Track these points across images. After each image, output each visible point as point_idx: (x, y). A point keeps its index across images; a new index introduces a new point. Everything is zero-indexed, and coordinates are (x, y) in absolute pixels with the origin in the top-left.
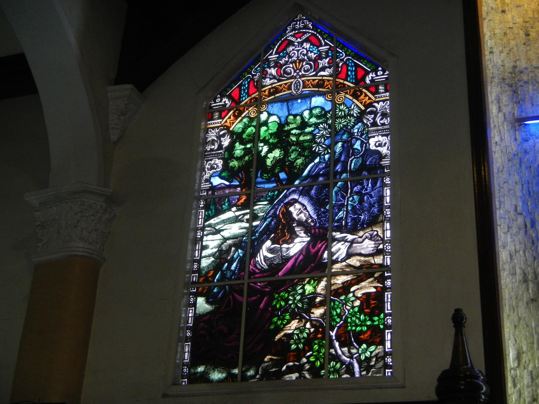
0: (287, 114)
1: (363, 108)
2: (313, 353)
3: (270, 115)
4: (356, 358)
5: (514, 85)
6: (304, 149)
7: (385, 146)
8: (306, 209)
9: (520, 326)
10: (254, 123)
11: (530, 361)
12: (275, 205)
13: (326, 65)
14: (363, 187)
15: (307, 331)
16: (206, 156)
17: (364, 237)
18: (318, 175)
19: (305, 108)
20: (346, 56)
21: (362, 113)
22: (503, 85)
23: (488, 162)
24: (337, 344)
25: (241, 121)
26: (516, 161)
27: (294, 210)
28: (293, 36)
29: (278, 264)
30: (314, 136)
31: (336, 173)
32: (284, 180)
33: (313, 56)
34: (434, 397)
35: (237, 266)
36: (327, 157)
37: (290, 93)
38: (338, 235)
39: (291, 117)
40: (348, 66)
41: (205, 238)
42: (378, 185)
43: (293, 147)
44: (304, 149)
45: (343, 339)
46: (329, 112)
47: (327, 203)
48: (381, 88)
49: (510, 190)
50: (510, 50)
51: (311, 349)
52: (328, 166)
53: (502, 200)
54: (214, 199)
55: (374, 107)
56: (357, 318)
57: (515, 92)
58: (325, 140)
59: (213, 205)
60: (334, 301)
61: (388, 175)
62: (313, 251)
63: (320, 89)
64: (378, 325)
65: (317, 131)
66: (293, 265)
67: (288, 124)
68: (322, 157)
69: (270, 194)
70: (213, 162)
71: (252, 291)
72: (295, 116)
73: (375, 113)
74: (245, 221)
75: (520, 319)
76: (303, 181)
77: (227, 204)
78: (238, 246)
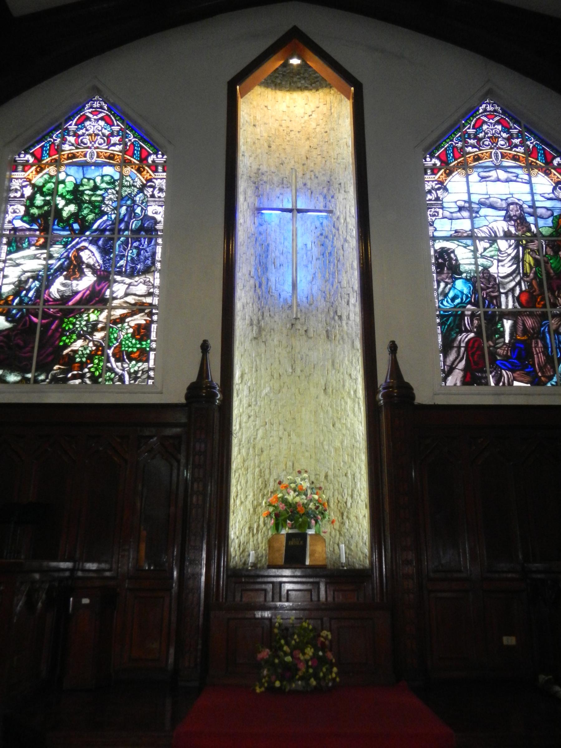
0: (82, 177)
1: (145, 182)
2: (94, 365)
3: (68, 175)
4: (127, 371)
5: (257, 183)
6: (95, 207)
7: (159, 214)
8: (94, 255)
9: (245, 356)
10: (54, 180)
11: (249, 380)
12: (69, 249)
13: (117, 142)
14: (141, 244)
15: (90, 349)
16: (8, 201)
17: (139, 281)
18: (105, 230)
19: (97, 174)
20: (134, 137)
21: (144, 186)
22: (249, 181)
23: (235, 238)
24: (112, 360)
25: (42, 176)
26: (253, 239)
27: (85, 256)
28: (91, 113)
29: (69, 296)
30: (104, 198)
31: (120, 230)
32: (77, 230)
33: (107, 133)
34: (183, 401)
35: (33, 294)
36: (113, 216)
37: (86, 160)
38: (118, 278)
39: (85, 180)
40: (134, 146)
41: (6, 269)
42: (153, 243)
43: (86, 205)
44: (95, 207)
45: (117, 356)
46: (117, 180)
47: (111, 253)
48: (160, 169)
49: (247, 259)
50: (257, 156)
51: (92, 362)
52: (113, 223)
53: (241, 266)
54: (16, 238)
55: (153, 182)
56: (129, 341)
57: (257, 188)
58: (113, 203)
59: (14, 243)
60: (112, 328)
61: (161, 236)
62: (98, 288)
63: (111, 161)
64: (145, 348)
65: (106, 194)
66: (81, 298)
67: (82, 185)
68: (109, 216)
69: (64, 240)
70: (15, 207)
71: (46, 315)
72: (89, 179)
73: (154, 187)
74: (42, 259)
75: (245, 350)
76: (92, 232)
77: (27, 244)
78: (35, 278)
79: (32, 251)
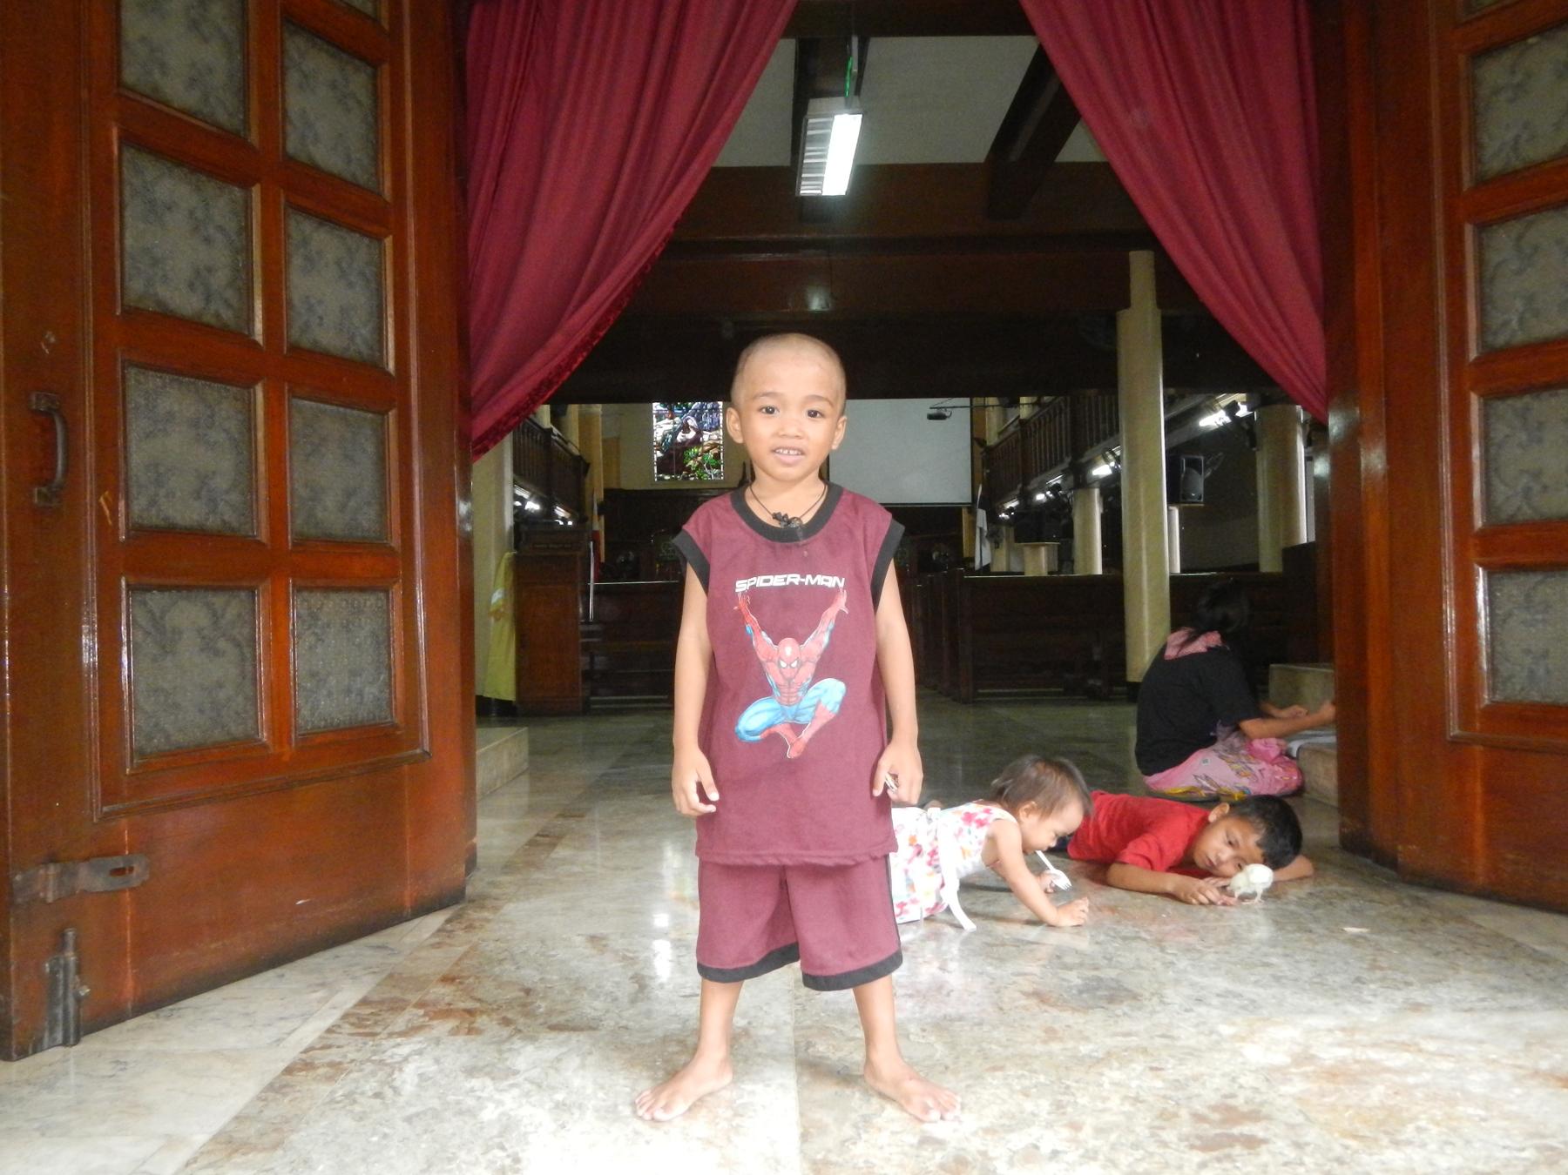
79: (667, 421)
